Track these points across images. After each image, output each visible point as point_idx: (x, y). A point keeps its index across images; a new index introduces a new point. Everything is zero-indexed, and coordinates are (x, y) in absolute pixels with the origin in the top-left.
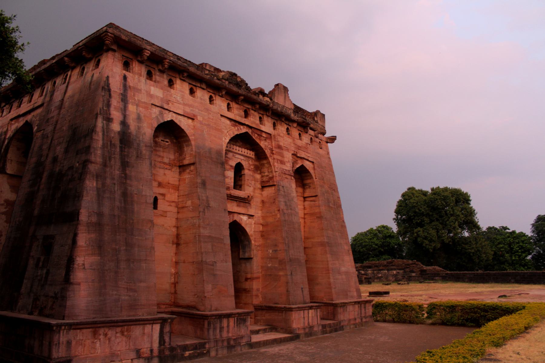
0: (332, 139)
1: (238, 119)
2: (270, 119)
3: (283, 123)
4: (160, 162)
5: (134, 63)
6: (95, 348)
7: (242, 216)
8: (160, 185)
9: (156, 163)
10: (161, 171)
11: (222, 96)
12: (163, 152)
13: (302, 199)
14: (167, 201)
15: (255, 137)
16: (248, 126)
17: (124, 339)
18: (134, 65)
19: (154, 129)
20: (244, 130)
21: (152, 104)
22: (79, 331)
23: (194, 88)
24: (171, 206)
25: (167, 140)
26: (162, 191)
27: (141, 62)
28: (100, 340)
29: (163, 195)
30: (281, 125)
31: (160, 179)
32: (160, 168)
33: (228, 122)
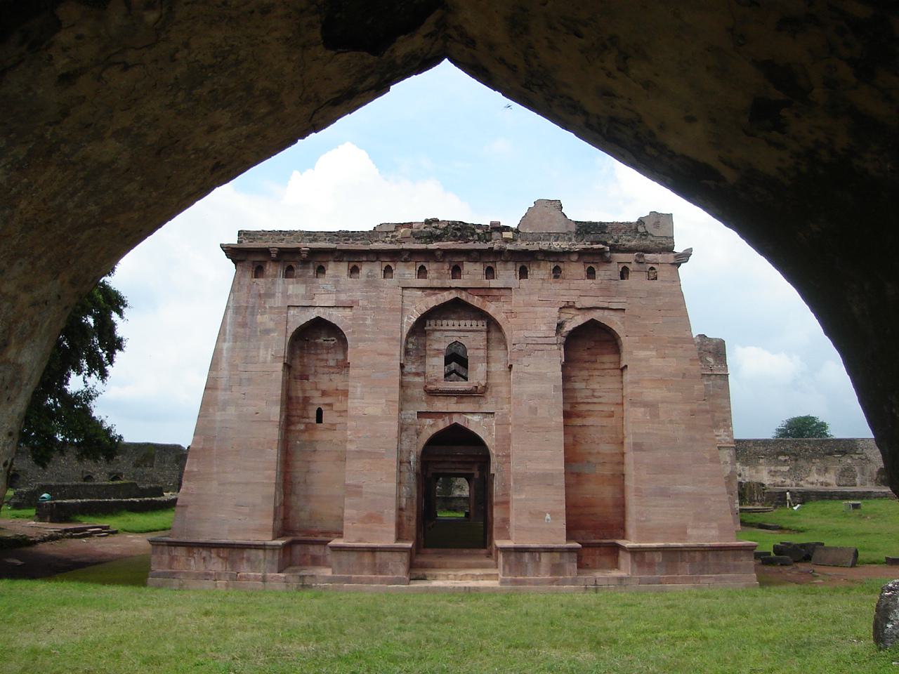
0: (686, 256)
1: (436, 284)
2: (511, 265)
3: (542, 263)
4: (324, 367)
5: (268, 265)
6: (189, 565)
7: (469, 417)
8: (324, 393)
9: (318, 369)
10: (326, 378)
11: (406, 261)
12: (328, 353)
13: (618, 372)
14: (336, 411)
15: (476, 301)
16: (456, 288)
17: (220, 560)
18: (267, 268)
19: (289, 335)
20: (447, 296)
21: (289, 306)
22: (173, 548)
23: (358, 264)
24: (342, 416)
25: (333, 338)
26: (328, 400)
27: (274, 261)
28: (194, 558)
29: (330, 405)
30: (539, 267)
31: (323, 387)
32: (323, 374)
33: (419, 293)
